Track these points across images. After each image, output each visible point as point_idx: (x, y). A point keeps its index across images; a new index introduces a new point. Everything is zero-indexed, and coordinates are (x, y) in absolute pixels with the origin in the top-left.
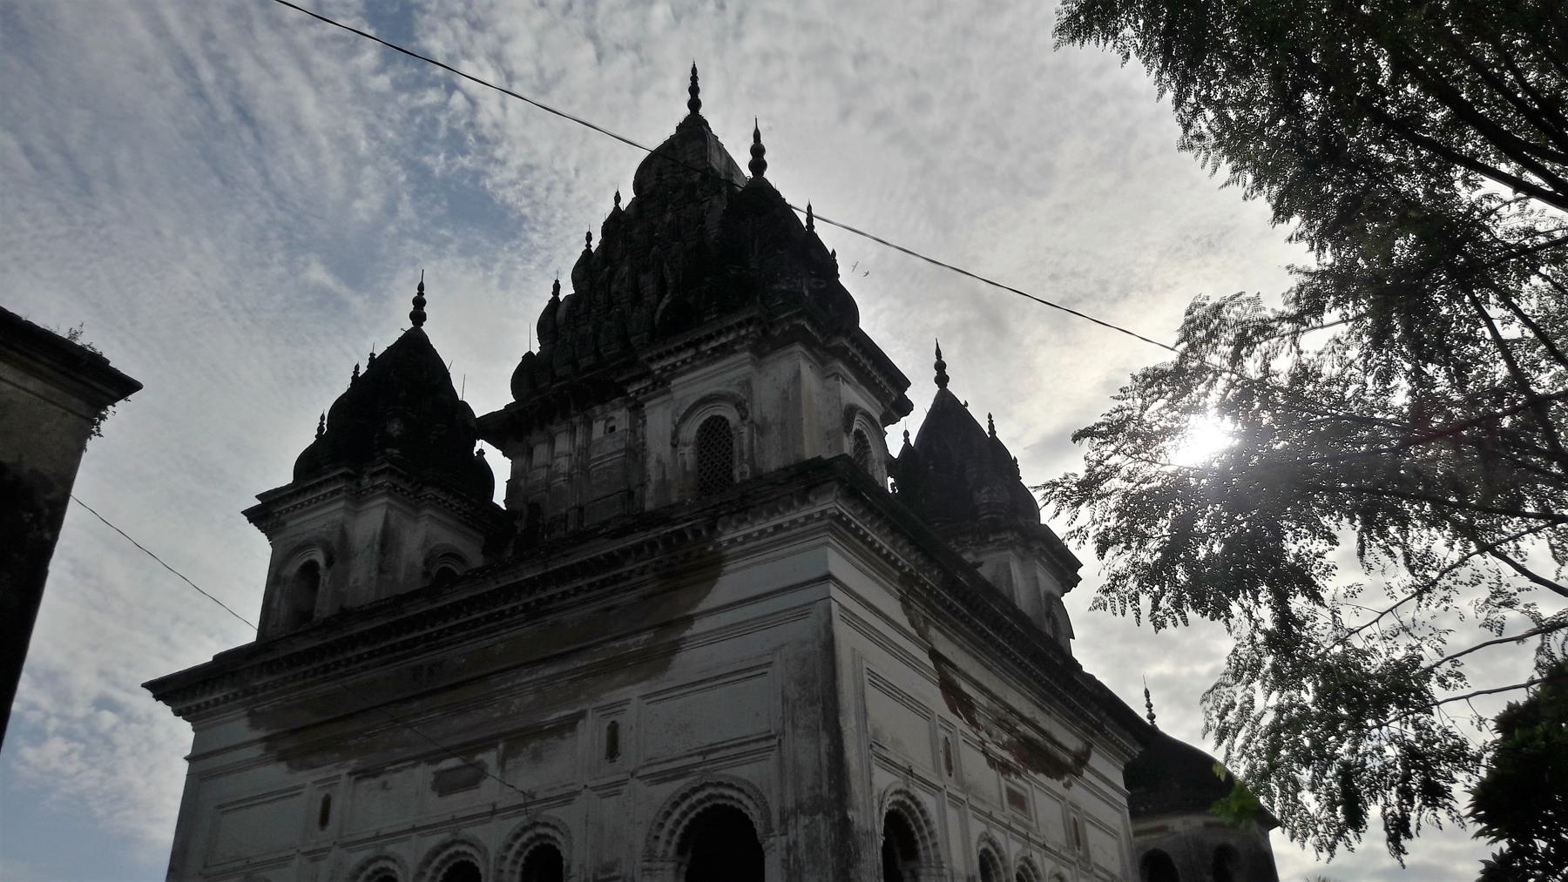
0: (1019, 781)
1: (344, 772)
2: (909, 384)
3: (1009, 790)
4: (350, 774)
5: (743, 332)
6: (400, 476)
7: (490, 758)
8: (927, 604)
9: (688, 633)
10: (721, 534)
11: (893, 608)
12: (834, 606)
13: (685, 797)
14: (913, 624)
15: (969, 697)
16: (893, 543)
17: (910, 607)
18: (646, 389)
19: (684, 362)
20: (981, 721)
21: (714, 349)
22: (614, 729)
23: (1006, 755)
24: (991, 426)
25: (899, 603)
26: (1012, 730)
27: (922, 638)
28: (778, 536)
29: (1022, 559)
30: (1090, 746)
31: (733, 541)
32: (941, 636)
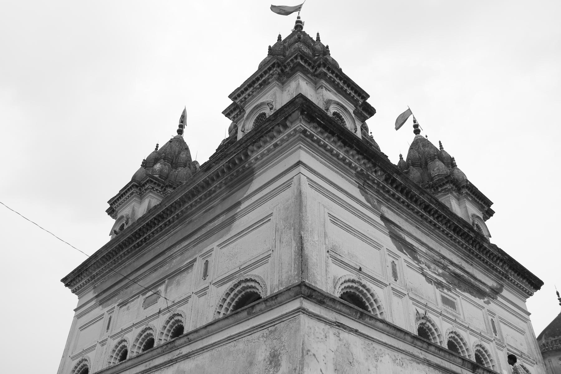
0: (449, 293)
1: (116, 305)
2: (368, 96)
3: (443, 297)
4: (118, 305)
5: (271, 72)
6: (155, 183)
7: (162, 288)
8: (378, 192)
9: (239, 210)
10: (250, 157)
11: (356, 192)
12: (303, 178)
13: (232, 290)
14: (368, 201)
15: (412, 245)
16: (347, 152)
17: (367, 193)
18: (237, 114)
19: (249, 95)
20: (422, 260)
21: (261, 85)
22: (207, 263)
23: (441, 279)
24: (441, 146)
25: (358, 190)
26: (444, 268)
27: (375, 209)
28: (277, 150)
29: (458, 199)
30: (502, 286)
31: (257, 159)
32: (390, 212)
